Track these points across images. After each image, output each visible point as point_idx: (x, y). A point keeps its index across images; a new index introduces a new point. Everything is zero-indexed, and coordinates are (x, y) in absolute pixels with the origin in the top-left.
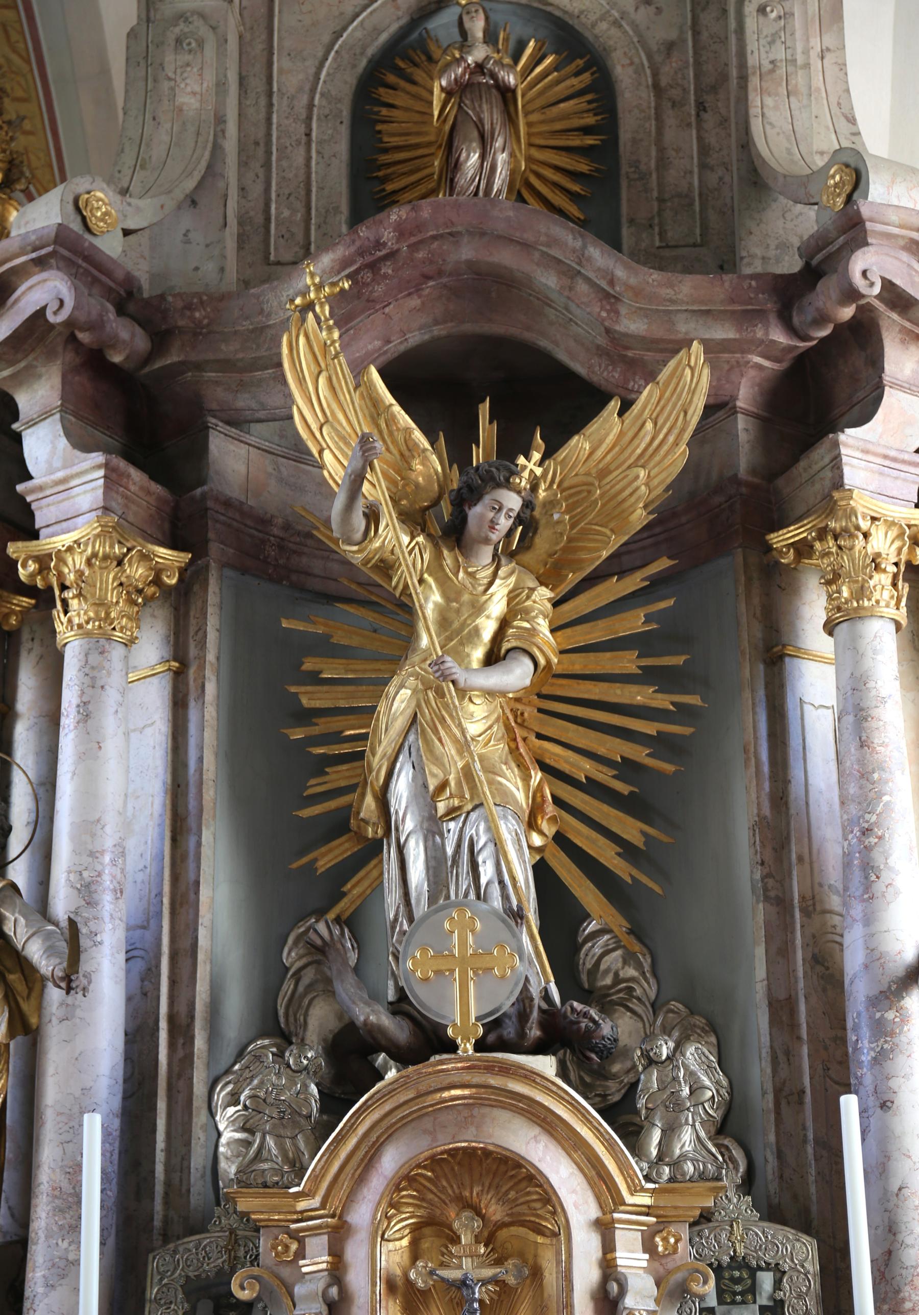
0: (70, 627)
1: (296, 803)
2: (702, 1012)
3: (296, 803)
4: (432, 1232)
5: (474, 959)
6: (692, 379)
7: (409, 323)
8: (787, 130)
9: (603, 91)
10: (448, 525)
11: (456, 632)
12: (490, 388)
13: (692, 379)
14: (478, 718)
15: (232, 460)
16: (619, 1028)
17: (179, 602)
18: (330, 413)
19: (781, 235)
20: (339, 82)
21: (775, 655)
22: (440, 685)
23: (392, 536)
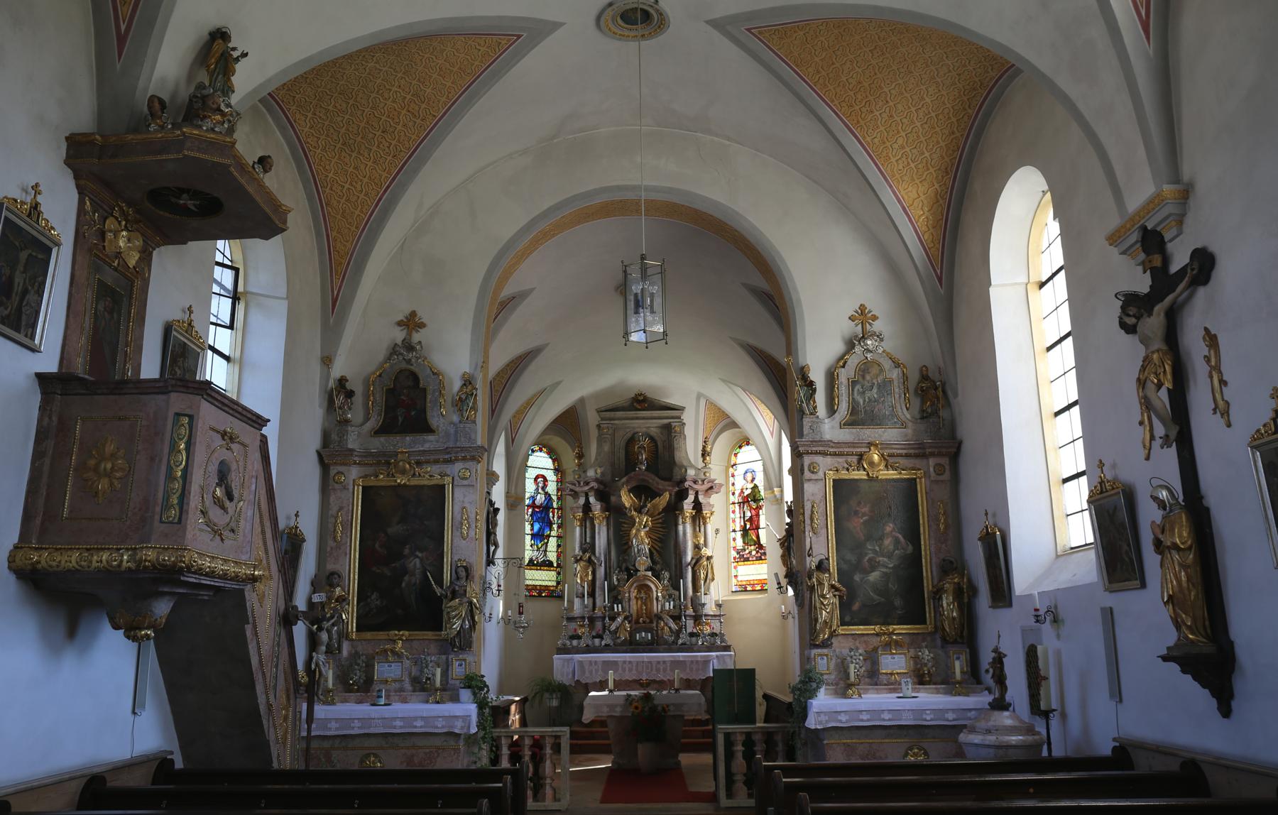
0: (596, 522)
1: (621, 541)
2: (667, 566)
3: (621, 541)
4: (639, 592)
5: (643, 562)
6: (667, 495)
7: (634, 484)
8: (678, 456)
9: (656, 446)
10: (639, 510)
11: (640, 523)
12: (644, 492)
13: (667, 495)
14: (642, 533)
15: (613, 499)
16: (658, 567)
17: (608, 519)
18: (627, 499)
19: (677, 477)
20: (623, 444)
21: (676, 525)
22: (638, 530)
23: (634, 513)
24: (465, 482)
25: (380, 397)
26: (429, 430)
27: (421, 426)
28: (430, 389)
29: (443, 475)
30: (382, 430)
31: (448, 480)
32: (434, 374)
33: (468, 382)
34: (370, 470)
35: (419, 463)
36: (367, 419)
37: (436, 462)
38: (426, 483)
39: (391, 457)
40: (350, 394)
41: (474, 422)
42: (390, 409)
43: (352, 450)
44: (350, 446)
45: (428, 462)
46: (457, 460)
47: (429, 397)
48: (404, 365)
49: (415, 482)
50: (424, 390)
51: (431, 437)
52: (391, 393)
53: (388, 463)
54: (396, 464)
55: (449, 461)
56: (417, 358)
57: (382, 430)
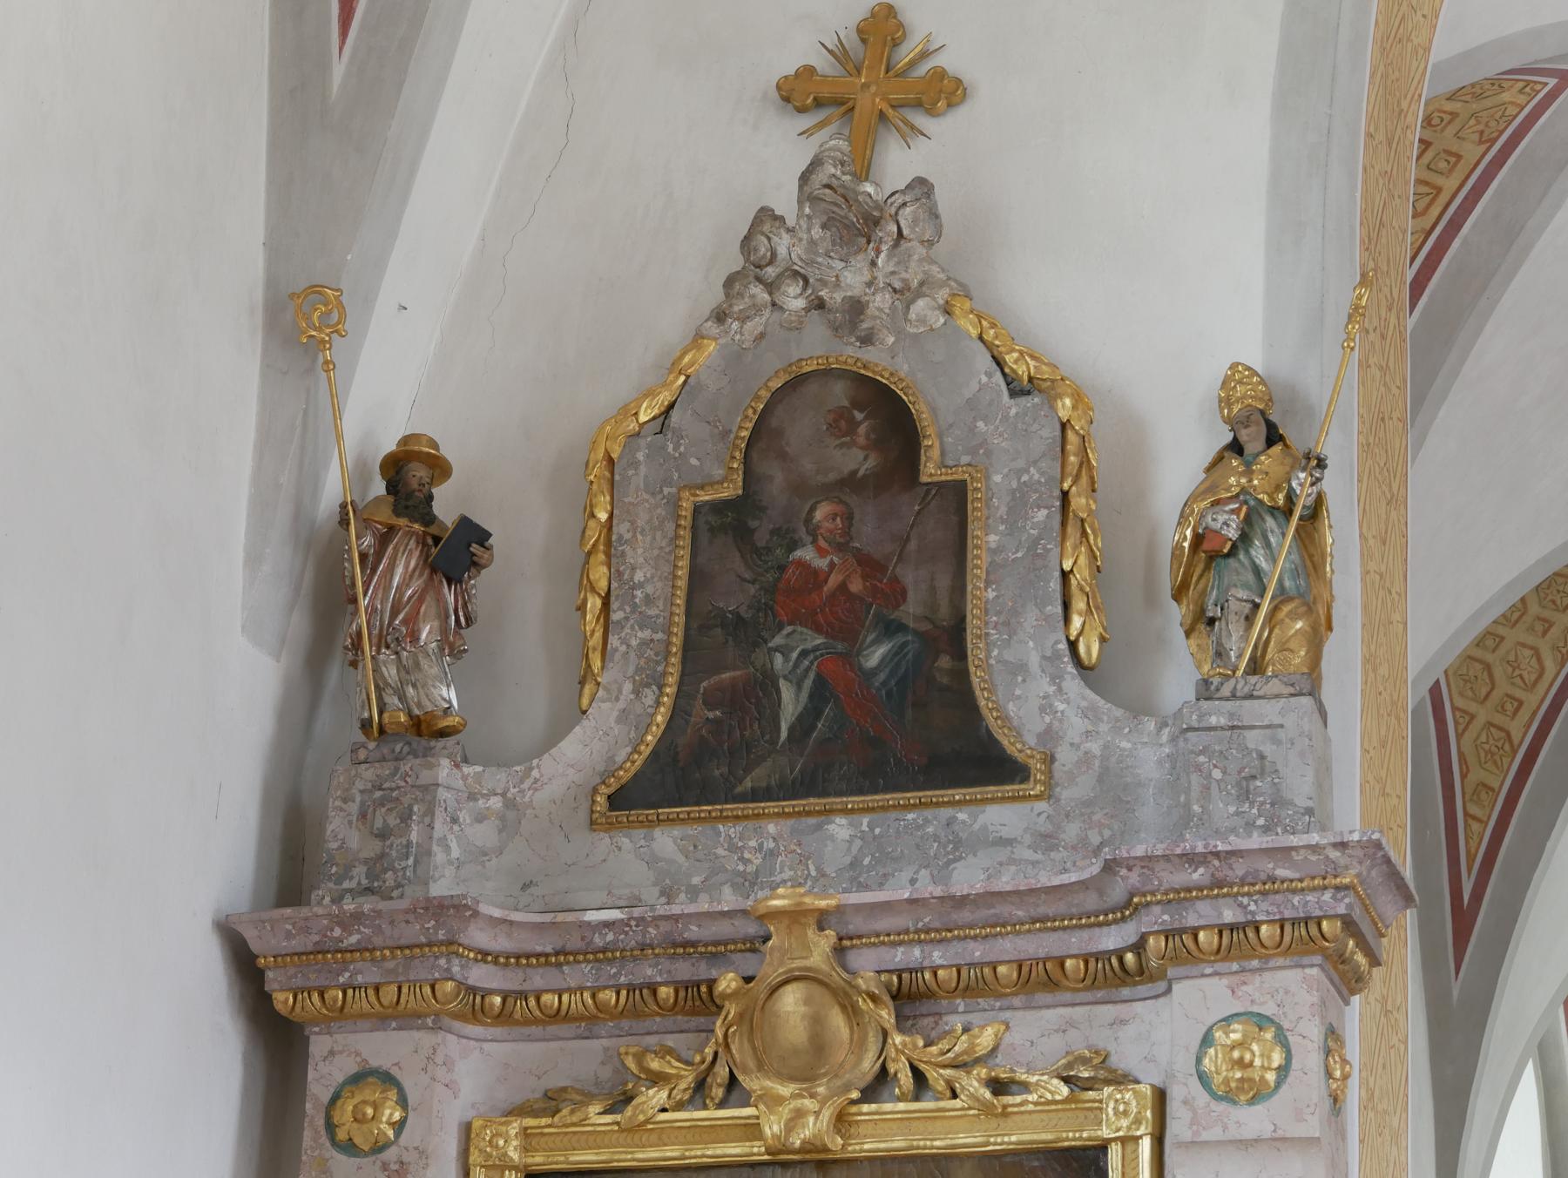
24: (1253, 1120)
25: (655, 568)
26: (985, 764)
27: (937, 740)
28: (997, 484)
29: (1089, 1075)
30: (671, 781)
31: (1117, 1116)
32: (1017, 389)
33: (1259, 426)
34: (577, 1058)
35: (910, 998)
36: (570, 714)
37: (1041, 980)
38: (968, 1138)
39: (717, 952)
40: (458, 553)
41: (1310, 684)
42: (717, 637)
43: (456, 909)
44: (439, 889)
45: (976, 986)
46: (1184, 950)
47: (987, 540)
48: (816, 345)
49: (889, 1129)
50: (956, 496)
51: (1000, 815)
52: (729, 524)
53: (699, 1001)
54: (758, 1003)
55: (1122, 975)
56: (905, 294)
57: (671, 781)
